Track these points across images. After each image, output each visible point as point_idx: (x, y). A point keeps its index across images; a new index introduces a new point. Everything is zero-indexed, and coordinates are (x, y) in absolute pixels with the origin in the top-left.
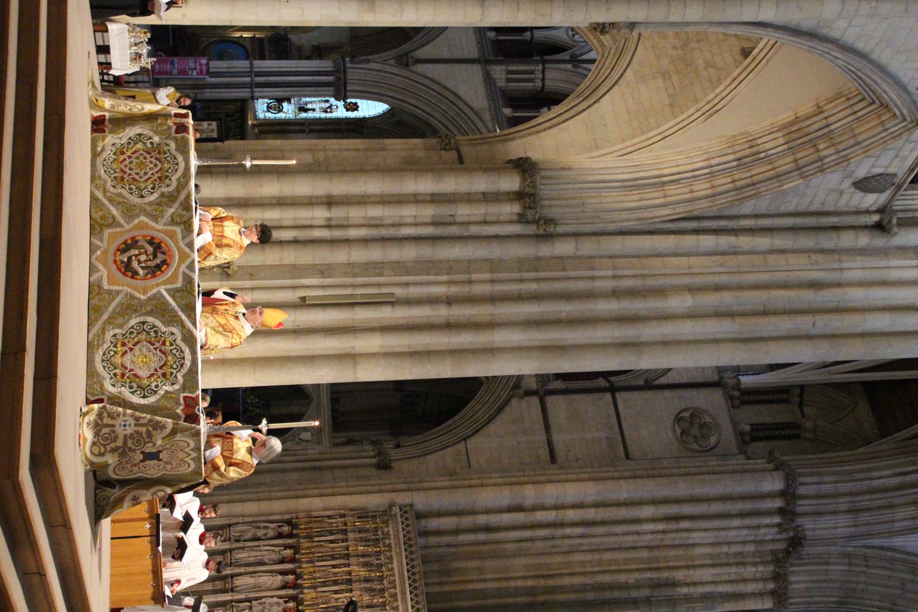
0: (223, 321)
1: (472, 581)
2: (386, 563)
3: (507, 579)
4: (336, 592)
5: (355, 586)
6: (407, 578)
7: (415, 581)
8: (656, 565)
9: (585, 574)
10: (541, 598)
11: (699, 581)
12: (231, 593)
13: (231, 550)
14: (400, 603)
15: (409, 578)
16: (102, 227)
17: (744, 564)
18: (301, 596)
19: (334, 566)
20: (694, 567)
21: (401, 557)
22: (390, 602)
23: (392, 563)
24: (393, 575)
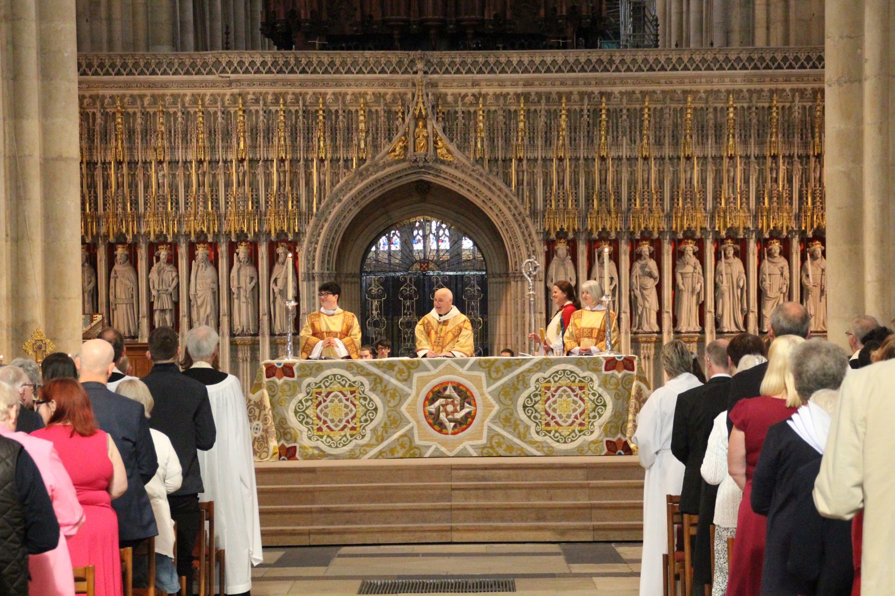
0: (450, 336)
4: (147, 187)
5: (139, 156)
6: (131, 77)
12: (260, 338)
13: (232, 335)
14: (169, 92)
15: (130, 73)
16: (412, 447)
18: (152, 237)
19: (106, 186)
21: (95, 82)
22: (164, 106)
23: (104, 97)
24: (123, 97)
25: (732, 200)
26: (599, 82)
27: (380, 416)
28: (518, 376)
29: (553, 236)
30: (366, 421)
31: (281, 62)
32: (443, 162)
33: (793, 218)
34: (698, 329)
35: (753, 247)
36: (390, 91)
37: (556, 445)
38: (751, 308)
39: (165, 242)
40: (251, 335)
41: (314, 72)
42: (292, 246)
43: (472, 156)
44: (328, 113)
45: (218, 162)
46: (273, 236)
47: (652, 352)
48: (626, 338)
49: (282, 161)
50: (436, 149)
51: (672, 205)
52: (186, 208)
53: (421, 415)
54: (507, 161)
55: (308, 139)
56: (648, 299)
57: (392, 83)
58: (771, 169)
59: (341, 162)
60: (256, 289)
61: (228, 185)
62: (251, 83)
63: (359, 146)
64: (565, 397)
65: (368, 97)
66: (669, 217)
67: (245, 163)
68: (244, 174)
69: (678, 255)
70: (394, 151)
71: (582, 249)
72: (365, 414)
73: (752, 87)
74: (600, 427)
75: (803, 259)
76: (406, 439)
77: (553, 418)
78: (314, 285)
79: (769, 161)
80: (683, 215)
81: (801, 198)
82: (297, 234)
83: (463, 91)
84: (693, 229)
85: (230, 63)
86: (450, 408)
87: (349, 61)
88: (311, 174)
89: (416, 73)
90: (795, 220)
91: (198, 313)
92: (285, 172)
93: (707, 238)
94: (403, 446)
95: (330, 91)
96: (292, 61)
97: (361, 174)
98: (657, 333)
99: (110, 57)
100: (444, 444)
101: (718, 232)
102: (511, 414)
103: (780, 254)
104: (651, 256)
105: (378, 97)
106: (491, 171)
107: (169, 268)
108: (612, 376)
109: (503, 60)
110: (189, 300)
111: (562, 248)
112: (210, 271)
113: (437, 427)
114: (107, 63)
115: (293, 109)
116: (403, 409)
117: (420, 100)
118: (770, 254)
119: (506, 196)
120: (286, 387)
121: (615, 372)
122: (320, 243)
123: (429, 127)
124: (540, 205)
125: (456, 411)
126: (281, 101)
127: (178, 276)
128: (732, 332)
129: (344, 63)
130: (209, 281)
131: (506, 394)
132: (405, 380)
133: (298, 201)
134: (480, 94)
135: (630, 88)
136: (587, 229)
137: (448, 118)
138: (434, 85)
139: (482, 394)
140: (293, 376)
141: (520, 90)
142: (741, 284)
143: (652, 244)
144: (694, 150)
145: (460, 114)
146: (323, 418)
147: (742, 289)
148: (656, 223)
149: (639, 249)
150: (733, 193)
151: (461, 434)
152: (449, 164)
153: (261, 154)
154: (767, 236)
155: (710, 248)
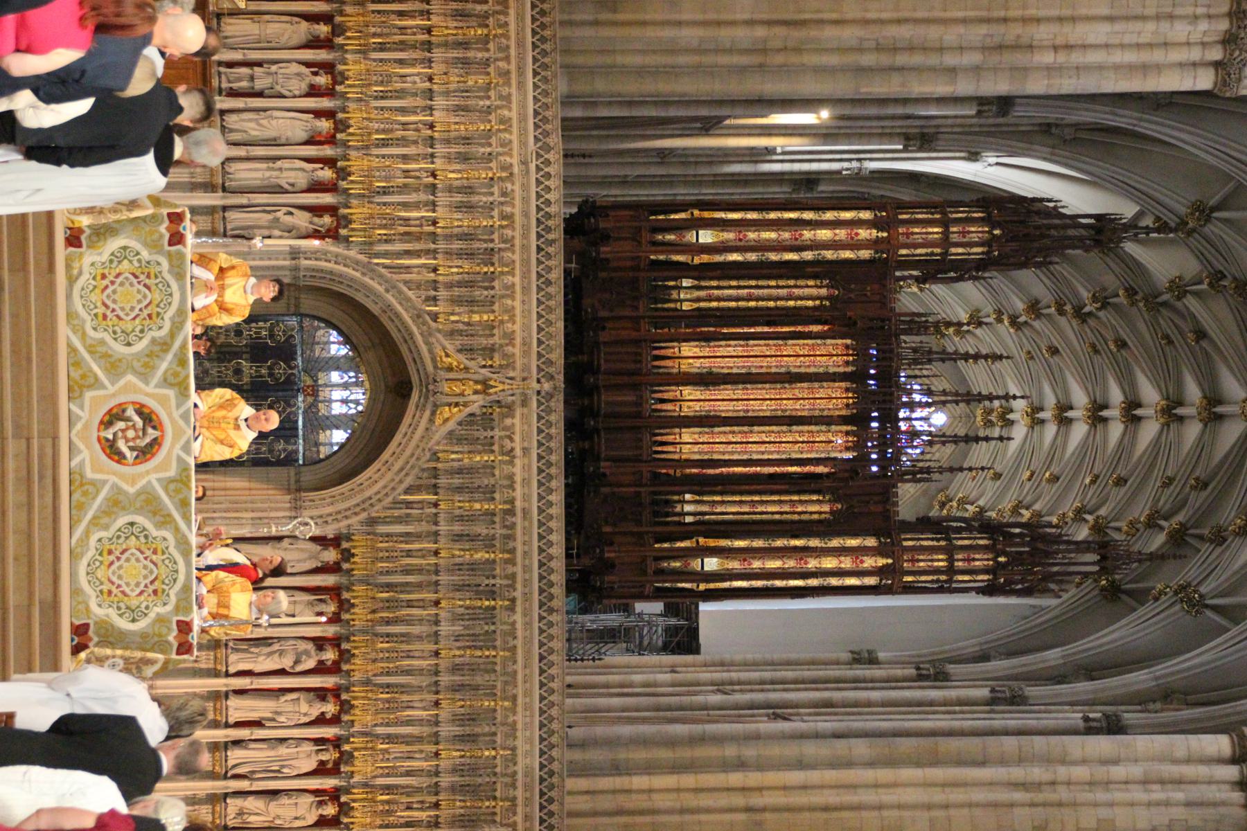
1: (654, 23)
2: (497, 13)
3: (719, 24)
4: (401, 62)
5: (437, 54)
6: (530, 47)
7: (544, 53)
8: (1002, 14)
9: (866, 22)
10: (779, 59)
11: (1080, 42)
12: (221, 194)
14: (514, 90)
15: (534, 46)
17: (1171, 17)
20: (1073, 19)
22: (497, 84)
23: (506, 14)
24: (507, 37)
26: (527, 597)
27: (119, 348)
28: (169, 515)
29: (345, 545)
30: (115, 332)
31: (550, 223)
32: (433, 413)
34: (231, 720)
35: (329, 783)
36: (517, 351)
37: (85, 562)
38: (256, 783)
39: (335, 82)
40: (223, 184)
41: (539, 262)
42: (331, 234)
43: (441, 448)
44: (491, 277)
45: (432, 147)
46: (343, 211)
47: (203, 666)
49: (434, 223)
50: (449, 405)
51: (381, 686)
52: (376, 108)
53: (122, 399)
54: (435, 489)
55: (460, 254)
57: (526, 353)
58: (422, 802)
59: (433, 293)
60: (280, 190)
61: (405, 158)
62: (525, 187)
63: (453, 314)
64: (145, 572)
65: (510, 325)
66: (367, 682)
67: (431, 180)
68: (418, 178)
69: (320, 694)
70: (447, 355)
71: (329, 580)
72: (123, 332)
73: (520, 776)
74: (107, 616)
76: (92, 380)
77: (118, 559)
78: (285, 259)
79: (433, 799)
80: (369, 699)
82: (346, 239)
83: (517, 438)
85: (548, 163)
86: (131, 434)
87: (552, 303)
88: (419, 257)
89: (539, 381)
91: (250, 120)
92: (421, 226)
93: (341, 728)
94: (83, 377)
95: (517, 280)
96: (551, 236)
97: (419, 316)
99: (552, 23)
100: (86, 427)
102: (124, 508)
103: (321, 816)
104: (321, 662)
105: (510, 337)
106: (423, 470)
107: (304, 87)
108: (170, 629)
109: (554, 484)
110: (265, 110)
111: (331, 555)
112: (303, 136)
113: (107, 418)
114: (546, 20)
115: (496, 236)
116: (130, 378)
117: (506, 387)
118: (321, 803)
119: (393, 489)
120: (155, 236)
121: (175, 632)
122: (336, 267)
123: (475, 397)
124: (382, 529)
125: (127, 441)
126: (505, 223)
127: (295, 97)
129: (549, 297)
130: (289, 134)
131: (148, 502)
132: (165, 380)
133: (386, 241)
134: (514, 457)
135: (519, 633)
137: (485, 419)
138: (524, 403)
139: (148, 472)
140: (170, 245)
141: (519, 504)
142: (285, 770)
143: (335, 662)
144: (444, 714)
145: (490, 433)
146: (119, 280)
147: (278, 771)
148: (359, 667)
149: (328, 647)
151: (98, 447)
152: (431, 421)
153: (442, 198)
154: (343, 799)
155: (329, 732)
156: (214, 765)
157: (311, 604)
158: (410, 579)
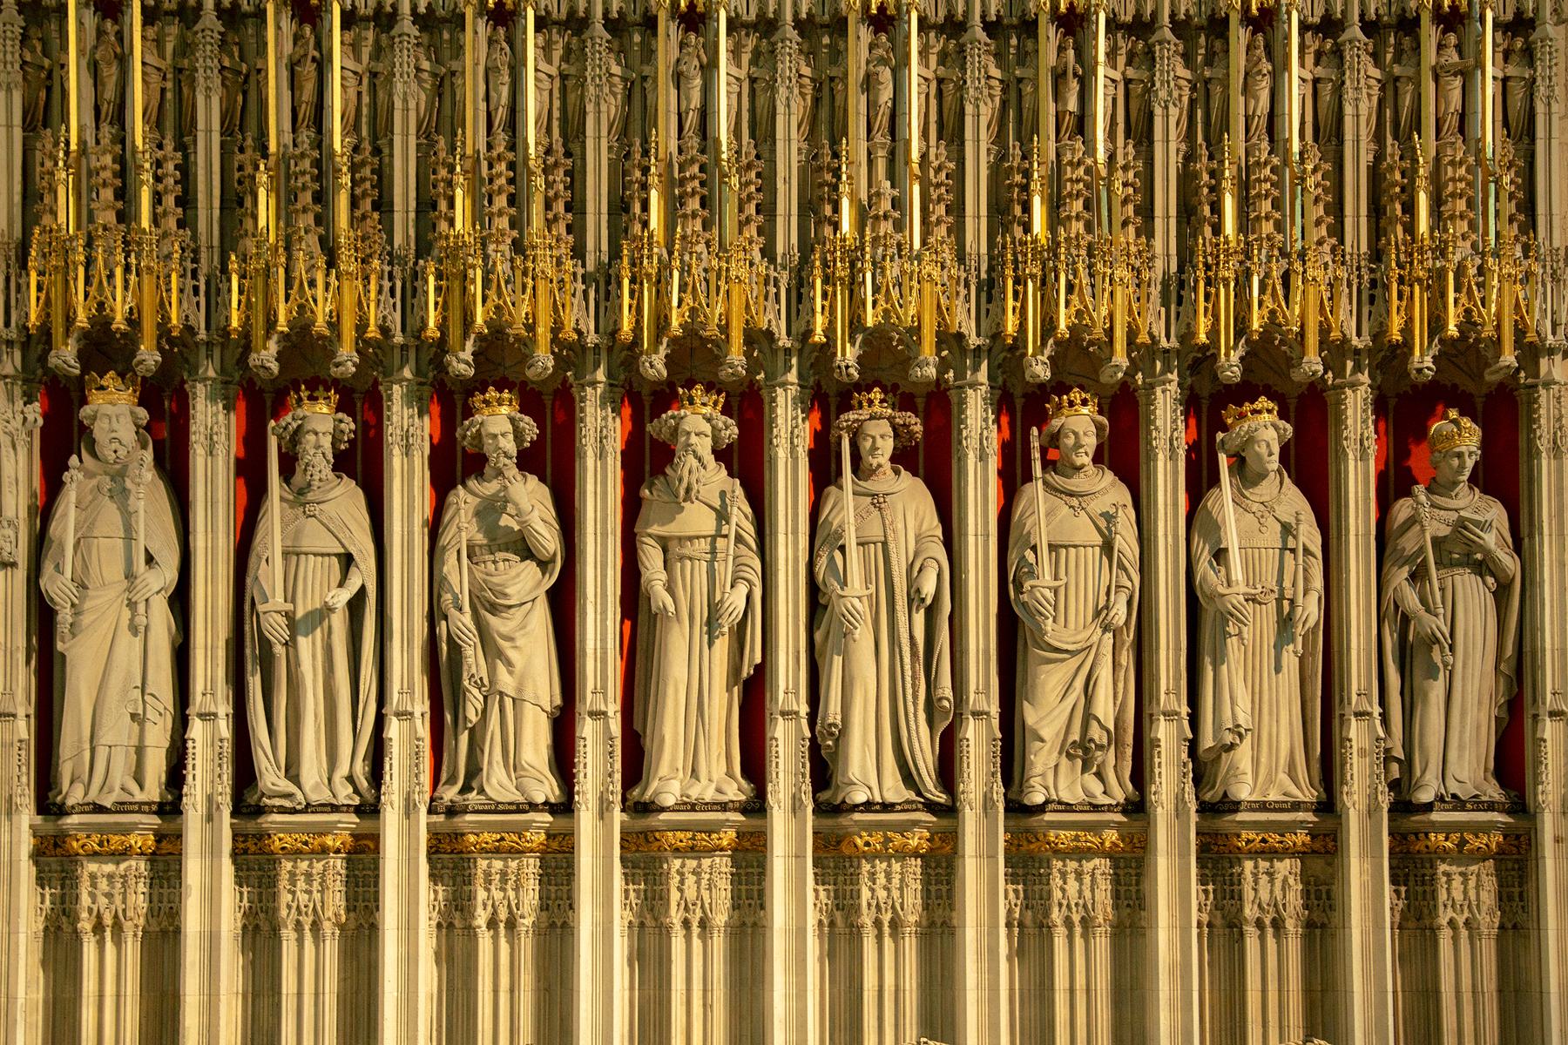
25: (886, 205)
29: (66, 355)
33: (1155, 291)
34: (737, 790)
38: (974, 700)
47: (530, 897)
48: (410, 834)
51: (618, 232)
56: (512, 654)
58: (1059, 77)
66: (604, 284)
75: (1200, 480)
79: (1049, 36)
80: (665, 267)
81: (1187, 212)
84: (712, 331)
90: (1165, 303)
93: (773, 381)
98: (550, 807)
101: (827, 348)
103: (1097, 459)
104: (528, 461)
128: (887, 807)
136: (225, 332)
142: (929, 588)
143: (530, 401)
147: (931, 613)
149: (466, 431)
150: (891, 176)
154: (1041, 370)
156: (902, 854)
157: (300, 496)
158: (209, 112)
